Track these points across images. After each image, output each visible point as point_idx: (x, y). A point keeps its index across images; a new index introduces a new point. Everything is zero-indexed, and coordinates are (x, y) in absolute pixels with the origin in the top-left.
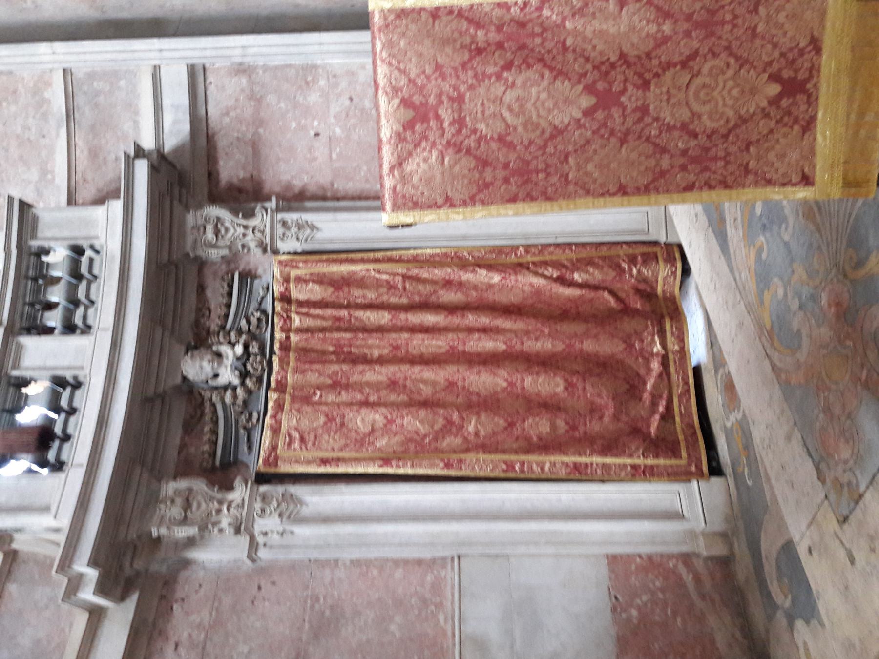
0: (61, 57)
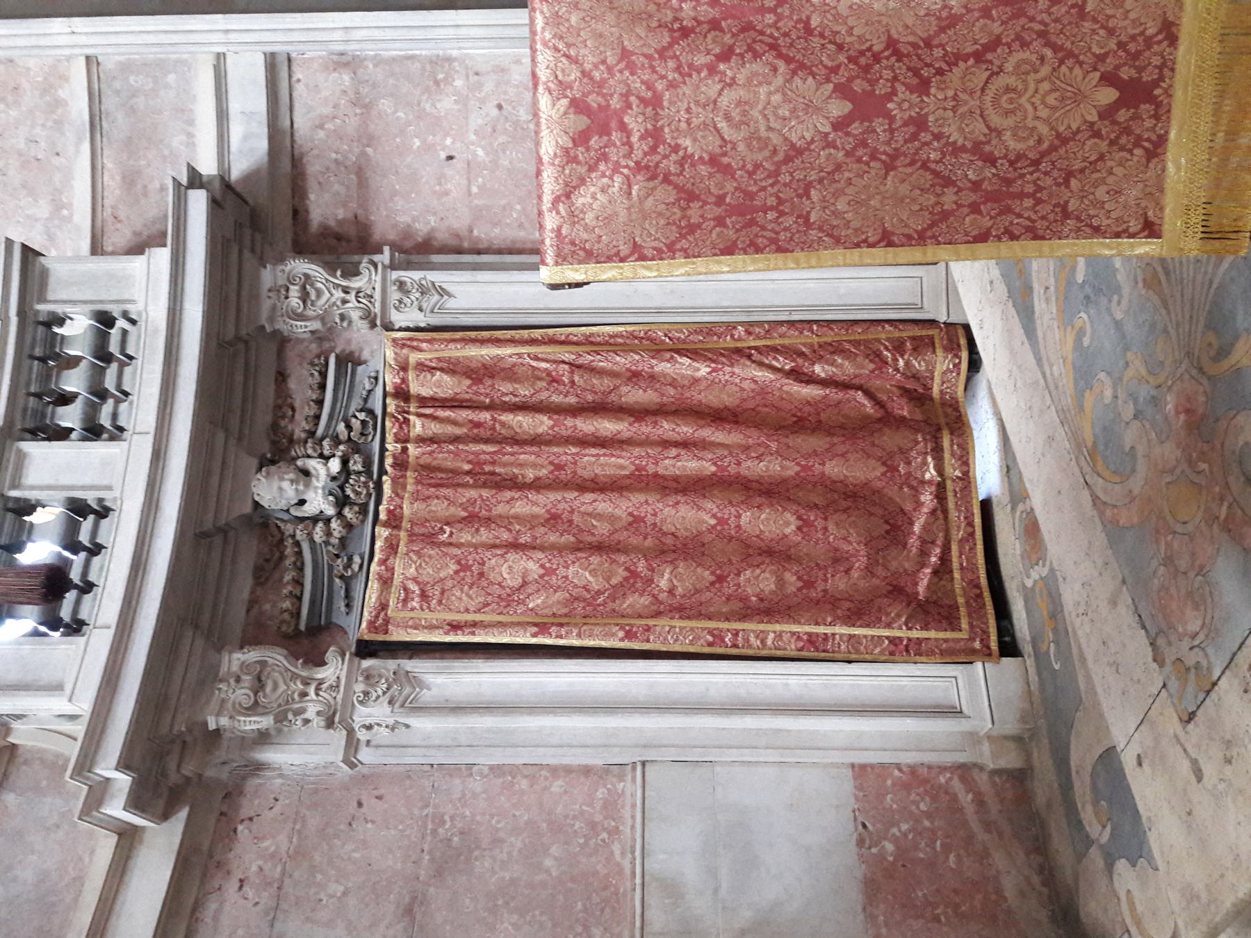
0: (83, 40)
